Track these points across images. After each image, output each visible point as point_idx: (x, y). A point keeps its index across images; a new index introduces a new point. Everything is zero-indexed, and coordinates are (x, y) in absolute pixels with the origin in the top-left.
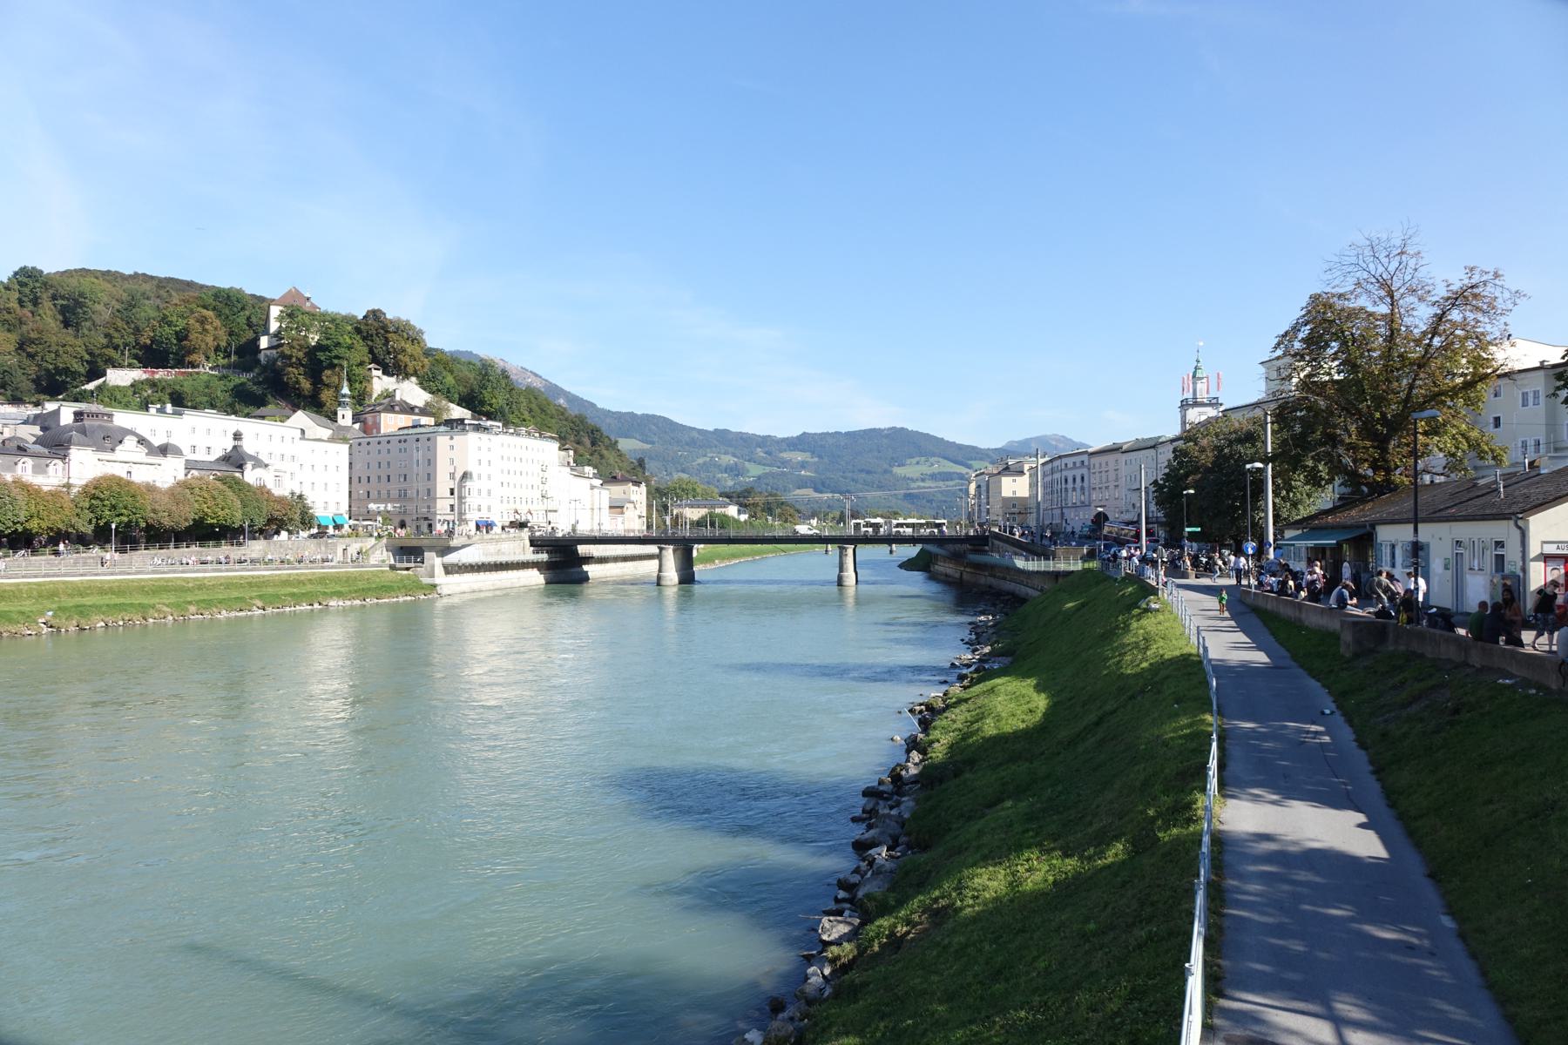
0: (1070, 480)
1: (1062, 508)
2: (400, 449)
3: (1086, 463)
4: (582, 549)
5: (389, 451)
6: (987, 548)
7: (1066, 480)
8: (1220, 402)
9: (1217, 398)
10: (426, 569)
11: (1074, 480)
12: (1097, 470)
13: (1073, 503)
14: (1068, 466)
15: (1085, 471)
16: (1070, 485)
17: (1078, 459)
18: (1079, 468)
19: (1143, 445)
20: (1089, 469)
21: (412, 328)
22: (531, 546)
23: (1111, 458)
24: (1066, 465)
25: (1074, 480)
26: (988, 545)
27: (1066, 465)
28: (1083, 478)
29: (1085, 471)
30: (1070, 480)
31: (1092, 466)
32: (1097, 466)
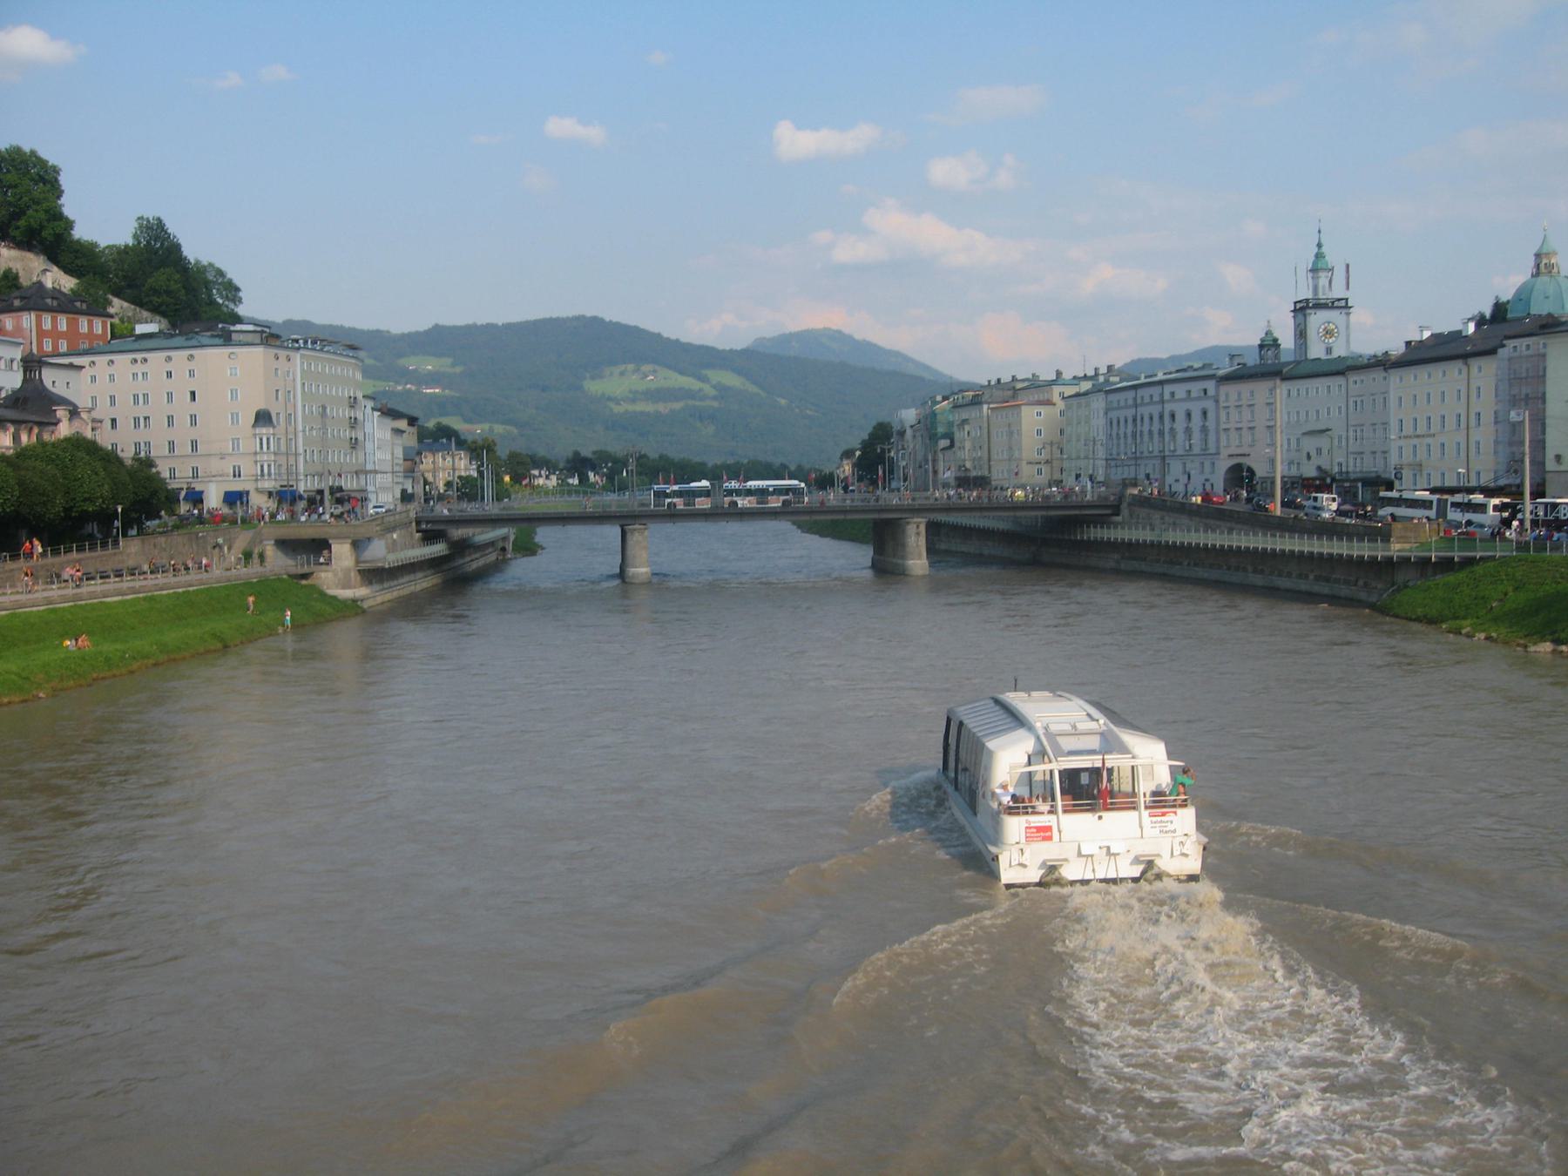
0: (1180, 417)
1: (1164, 458)
2: (135, 375)
3: (1211, 392)
4: (457, 533)
5: (112, 378)
6: (1119, 519)
7: (1173, 416)
8: (1349, 305)
9: (1347, 299)
10: (336, 575)
11: (1189, 415)
12: (1232, 402)
13: (1150, 452)
14: (1176, 397)
15: (1209, 405)
16: (1180, 425)
17: (1196, 388)
18: (1198, 399)
19: (1326, 369)
20: (1217, 401)
21: (42, 163)
22: (418, 531)
23: (1261, 389)
24: (1173, 394)
25: (1189, 415)
26: (1118, 515)
27: (1173, 394)
28: (1205, 413)
29: (1209, 405)
30: (1180, 417)
31: (1222, 398)
32: (1233, 397)
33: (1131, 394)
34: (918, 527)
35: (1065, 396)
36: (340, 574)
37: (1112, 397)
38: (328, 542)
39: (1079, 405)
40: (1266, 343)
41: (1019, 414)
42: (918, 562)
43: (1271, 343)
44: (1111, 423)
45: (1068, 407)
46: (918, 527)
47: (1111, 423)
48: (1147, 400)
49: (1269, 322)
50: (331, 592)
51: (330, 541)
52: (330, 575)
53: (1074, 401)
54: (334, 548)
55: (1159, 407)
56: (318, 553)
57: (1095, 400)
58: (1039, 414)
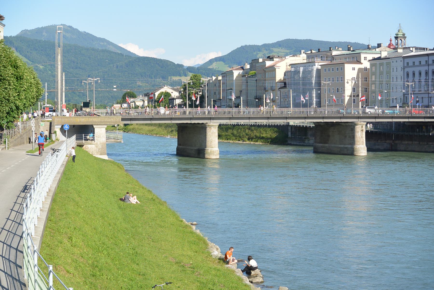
33: (426, 58)
34: (362, 127)
35: (368, 59)
36: (100, 146)
37: (406, 60)
38: (93, 127)
39: (381, 64)
40: (399, 36)
41: (343, 69)
42: (362, 146)
43: (402, 36)
44: (408, 75)
45: (371, 65)
46: (362, 127)
47: (408, 75)
48: (417, 63)
49: (400, 24)
50: (96, 156)
51: (94, 127)
52: (93, 146)
53: (378, 62)
54: (96, 130)
55: (426, 68)
56: (87, 133)
57: (395, 61)
58: (354, 69)
